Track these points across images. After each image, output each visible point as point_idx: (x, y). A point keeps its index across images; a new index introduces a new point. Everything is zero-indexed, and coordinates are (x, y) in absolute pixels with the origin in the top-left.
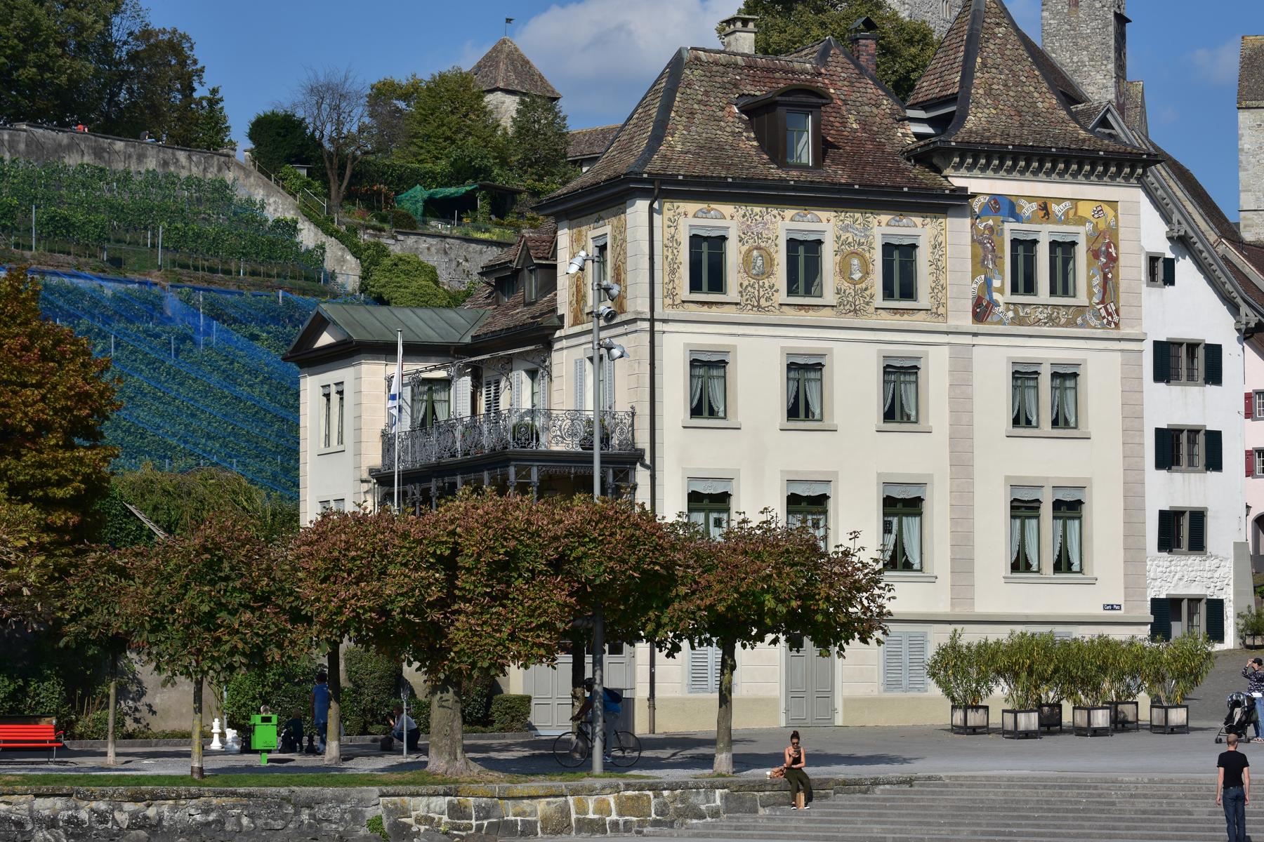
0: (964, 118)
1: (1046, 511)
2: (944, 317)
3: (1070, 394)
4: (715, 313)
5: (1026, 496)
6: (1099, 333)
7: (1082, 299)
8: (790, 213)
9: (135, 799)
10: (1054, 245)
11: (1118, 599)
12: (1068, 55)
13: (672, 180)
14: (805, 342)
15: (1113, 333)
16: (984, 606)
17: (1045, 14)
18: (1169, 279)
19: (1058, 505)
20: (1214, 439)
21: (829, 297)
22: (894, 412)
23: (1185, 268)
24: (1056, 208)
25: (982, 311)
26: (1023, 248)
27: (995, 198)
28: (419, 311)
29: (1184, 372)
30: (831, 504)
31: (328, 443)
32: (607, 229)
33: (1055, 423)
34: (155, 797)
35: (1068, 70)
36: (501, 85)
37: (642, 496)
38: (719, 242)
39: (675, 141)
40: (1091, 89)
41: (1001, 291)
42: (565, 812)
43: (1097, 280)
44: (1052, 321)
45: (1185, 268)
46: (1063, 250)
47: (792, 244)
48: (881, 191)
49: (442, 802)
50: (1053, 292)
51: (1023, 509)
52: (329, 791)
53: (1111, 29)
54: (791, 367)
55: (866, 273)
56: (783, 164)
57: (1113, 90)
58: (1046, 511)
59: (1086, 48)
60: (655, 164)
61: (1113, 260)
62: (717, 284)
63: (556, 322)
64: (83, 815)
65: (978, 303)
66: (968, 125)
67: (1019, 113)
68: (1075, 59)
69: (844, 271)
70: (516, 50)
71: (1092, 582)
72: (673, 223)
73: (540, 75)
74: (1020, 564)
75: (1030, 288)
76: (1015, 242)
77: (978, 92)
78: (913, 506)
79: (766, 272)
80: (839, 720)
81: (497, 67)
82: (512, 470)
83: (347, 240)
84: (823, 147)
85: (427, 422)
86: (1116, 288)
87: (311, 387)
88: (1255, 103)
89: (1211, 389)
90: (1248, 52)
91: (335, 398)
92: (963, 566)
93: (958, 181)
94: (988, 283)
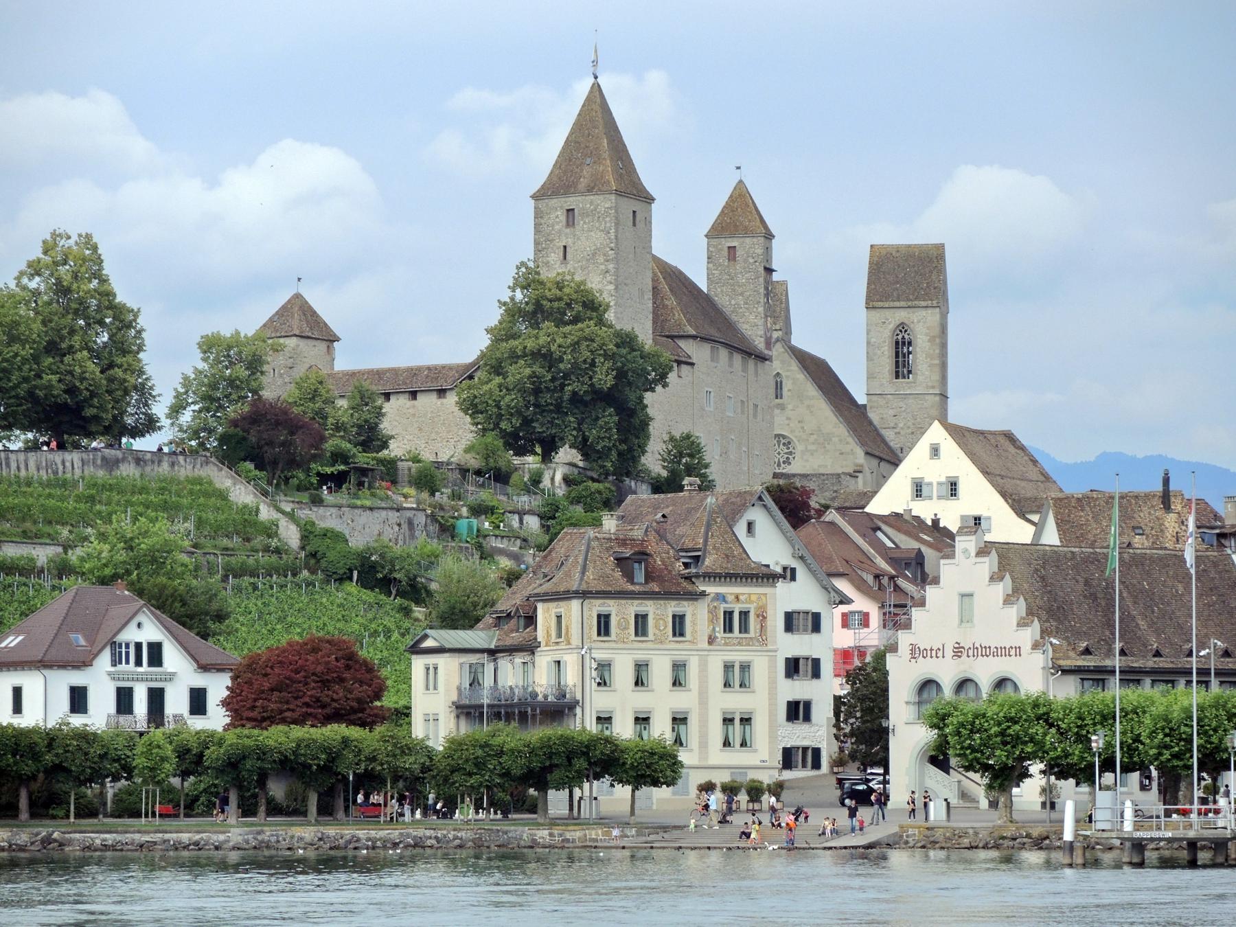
0: (704, 559)
1: (737, 722)
2: (696, 643)
3: (747, 674)
4: (606, 645)
5: (729, 716)
6: (759, 648)
7: (752, 634)
8: (636, 602)
9: (454, 830)
10: (741, 613)
11: (766, 758)
12: (727, 298)
13: (591, 592)
14: (641, 656)
15: (765, 648)
16: (713, 761)
17: (711, 265)
18: (793, 578)
19: (742, 720)
20: (816, 663)
21: (651, 636)
22: (676, 683)
23: (801, 573)
24: (741, 597)
25: (711, 640)
26: (729, 615)
27: (717, 594)
28: (467, 632)
29: (801, 627)
30: (651, 721)
31: (427, 689)
32: (562, 610)
33: (741, 686)
34: (460, 829)
35: (727, 310)
36: (297, 332)
37: (578, 720)
38: (607, 617)
39: (590, 575)
40: (745, 326)
41: (719, 632)
42: (585, 835)
43: (759, 627)
44: (739, 644)
45: (801, 573)
46: (744, 615)
47: (637, 616)
48: (672, 593)
49: (546, 832)
50: (740, 632)
51: (728, 721)
52: (512, 828)
53: (761, 279)
54: (636, 665)
55: (666, 627)
56: (633, 583)
57: (762, 328)
58: (737, 722)
59: (742, 294)
60: (584, 587)
61: (765, 618)
62: (607, 633)
63: (537, 644)
64: (439, 835)
65: (710, 637)
66: (706, 563)
67: (727, 556)
68: (733, 302)
69: (657, 627)
70: (307, 302)
71: (756, 751)
72: (590, 609)
73: (326, 325)
74: (727, 743)
75: (731, 630)
76: (725, 612)
77: (710, 548)
78: (684, 720)
79: (626, 628)
80: (654, 807)
81: (293, 317)
82: (529, 710)
83: (291, 516)
84: (649, 577)
85: (475, 683)
86: (766, 631)
87: (418, 664)
88: (881, 304)
89: (815, 636)
90: (876, 259)
91: (431, 671)
92: (704, 745)
93: (702, 588)
94: (714, 629)
